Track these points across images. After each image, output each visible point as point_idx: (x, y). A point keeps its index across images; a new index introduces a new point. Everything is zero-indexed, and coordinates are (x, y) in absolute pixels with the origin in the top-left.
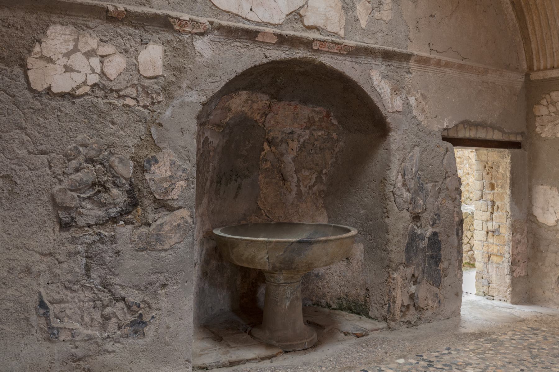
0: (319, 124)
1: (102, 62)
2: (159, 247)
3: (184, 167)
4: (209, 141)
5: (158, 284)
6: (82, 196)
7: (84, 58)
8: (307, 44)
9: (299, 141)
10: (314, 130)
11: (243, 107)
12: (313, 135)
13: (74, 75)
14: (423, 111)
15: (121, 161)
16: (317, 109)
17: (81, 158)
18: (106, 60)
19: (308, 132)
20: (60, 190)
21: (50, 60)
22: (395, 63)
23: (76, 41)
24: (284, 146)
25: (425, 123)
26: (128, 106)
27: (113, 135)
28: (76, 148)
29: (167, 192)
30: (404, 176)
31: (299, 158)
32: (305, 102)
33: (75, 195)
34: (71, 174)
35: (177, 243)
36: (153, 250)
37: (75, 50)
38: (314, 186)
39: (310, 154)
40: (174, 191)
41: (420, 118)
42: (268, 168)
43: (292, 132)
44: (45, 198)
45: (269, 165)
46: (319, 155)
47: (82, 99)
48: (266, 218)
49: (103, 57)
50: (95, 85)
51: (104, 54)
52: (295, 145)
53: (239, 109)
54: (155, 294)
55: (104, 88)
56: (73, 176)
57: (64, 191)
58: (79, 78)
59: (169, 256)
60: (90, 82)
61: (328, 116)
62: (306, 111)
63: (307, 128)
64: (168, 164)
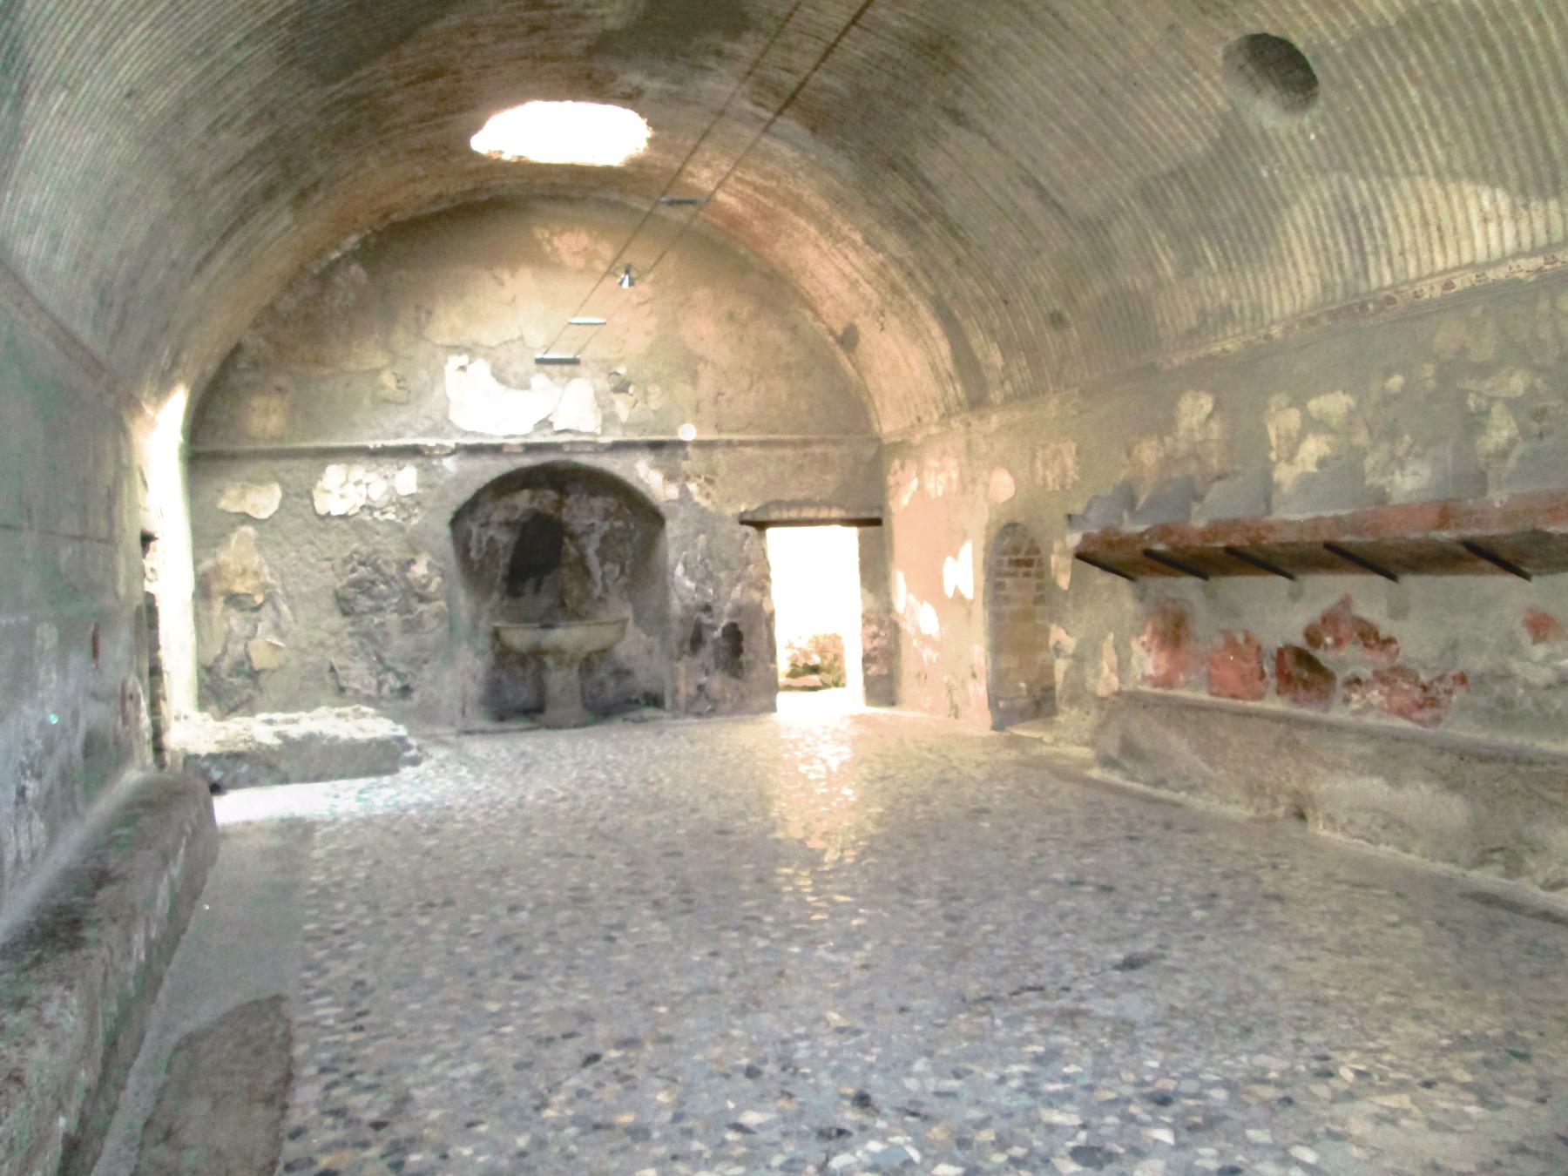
14: (708, 496)
21: (328, 492)
22: (666, 452)
25: (712, 509)
29: (425, 586)
41: (704, 503)
44: (331, 592)
52: (596, 537)
53: (528, 506)
54: (419, 669)
57: (344, 587)
61: (620, 506)
62: (598, 503)
63: (605, 519)
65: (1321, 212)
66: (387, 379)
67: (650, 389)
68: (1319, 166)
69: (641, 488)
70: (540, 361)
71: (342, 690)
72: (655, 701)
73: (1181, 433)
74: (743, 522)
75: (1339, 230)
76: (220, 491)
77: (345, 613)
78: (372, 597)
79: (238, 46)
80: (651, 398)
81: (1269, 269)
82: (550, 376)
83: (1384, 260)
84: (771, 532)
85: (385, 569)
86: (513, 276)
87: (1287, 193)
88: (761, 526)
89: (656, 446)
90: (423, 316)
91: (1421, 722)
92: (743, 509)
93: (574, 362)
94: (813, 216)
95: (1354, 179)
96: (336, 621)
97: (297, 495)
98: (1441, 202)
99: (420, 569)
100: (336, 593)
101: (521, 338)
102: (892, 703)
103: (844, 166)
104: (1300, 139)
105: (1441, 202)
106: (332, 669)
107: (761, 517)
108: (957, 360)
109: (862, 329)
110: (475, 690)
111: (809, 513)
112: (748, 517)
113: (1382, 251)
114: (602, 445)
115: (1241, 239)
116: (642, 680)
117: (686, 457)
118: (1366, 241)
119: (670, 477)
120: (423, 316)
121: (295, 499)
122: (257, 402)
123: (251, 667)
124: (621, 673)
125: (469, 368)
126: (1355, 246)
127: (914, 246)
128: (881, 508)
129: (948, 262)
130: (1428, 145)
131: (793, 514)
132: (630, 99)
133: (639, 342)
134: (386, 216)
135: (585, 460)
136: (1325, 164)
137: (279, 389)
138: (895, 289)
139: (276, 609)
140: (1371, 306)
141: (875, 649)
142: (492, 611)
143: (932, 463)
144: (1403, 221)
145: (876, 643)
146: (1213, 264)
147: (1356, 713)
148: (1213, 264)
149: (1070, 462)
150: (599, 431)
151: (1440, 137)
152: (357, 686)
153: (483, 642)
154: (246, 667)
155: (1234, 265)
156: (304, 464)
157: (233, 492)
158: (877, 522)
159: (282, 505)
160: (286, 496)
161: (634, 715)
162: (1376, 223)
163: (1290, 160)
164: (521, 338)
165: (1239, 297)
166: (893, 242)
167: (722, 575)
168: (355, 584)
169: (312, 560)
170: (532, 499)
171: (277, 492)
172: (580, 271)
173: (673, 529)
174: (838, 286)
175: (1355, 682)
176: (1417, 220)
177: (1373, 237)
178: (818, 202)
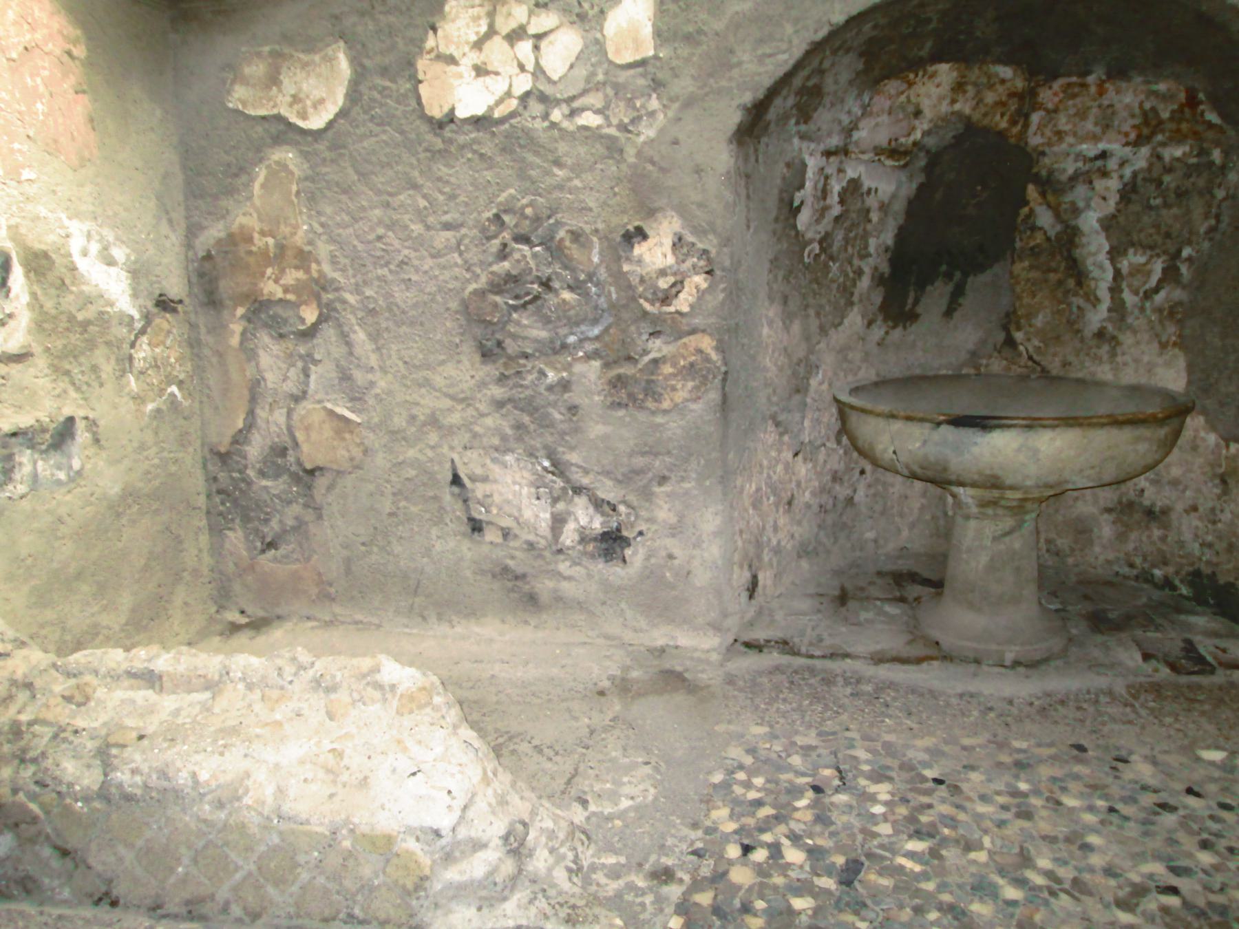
0: (1171, 126)
1: (536, 48)
2: (650, 404)
3: (700, 246)
4: (865, 188)
5: (650, 475)
6: (511, 302)
7: (505, 45)
9: (1121, 177)
10: (1163, 144)
11: (953, 101)
12: (1159, 157)
13: (488, 80)
16: (1162, 87)
17: (506, 235)
18: (544, 44)
19: (1145, 151)
20: (475, 292)
21: (451, 60)
26: (586, 128)
27: (560, 187)
28: (497, 217)
31: (1121, 219)
33: (498, 299)
34: (490, 264)
35: (687, 400)
36: (642, 408)
37: (491, 32)
38: (1156, 290)
39: (1150, 208)
40: (681, 296)
42: (1038, 246)
46: (1175, 211)
47: (507, 126)
48: (1030, 363)
49: (539, 37)
50: (527, 94)
51: (541, 31)
54: (647, 494)
55: (543, 98)
56: (495, 268)
58: (498, 86)
60: (518, 91)
64: (668, 242)
106: (456, 480)
139: (345, 339)
142: (843, 351)
159: (354, 95)
169: (417, 228)
171: (344, 65)
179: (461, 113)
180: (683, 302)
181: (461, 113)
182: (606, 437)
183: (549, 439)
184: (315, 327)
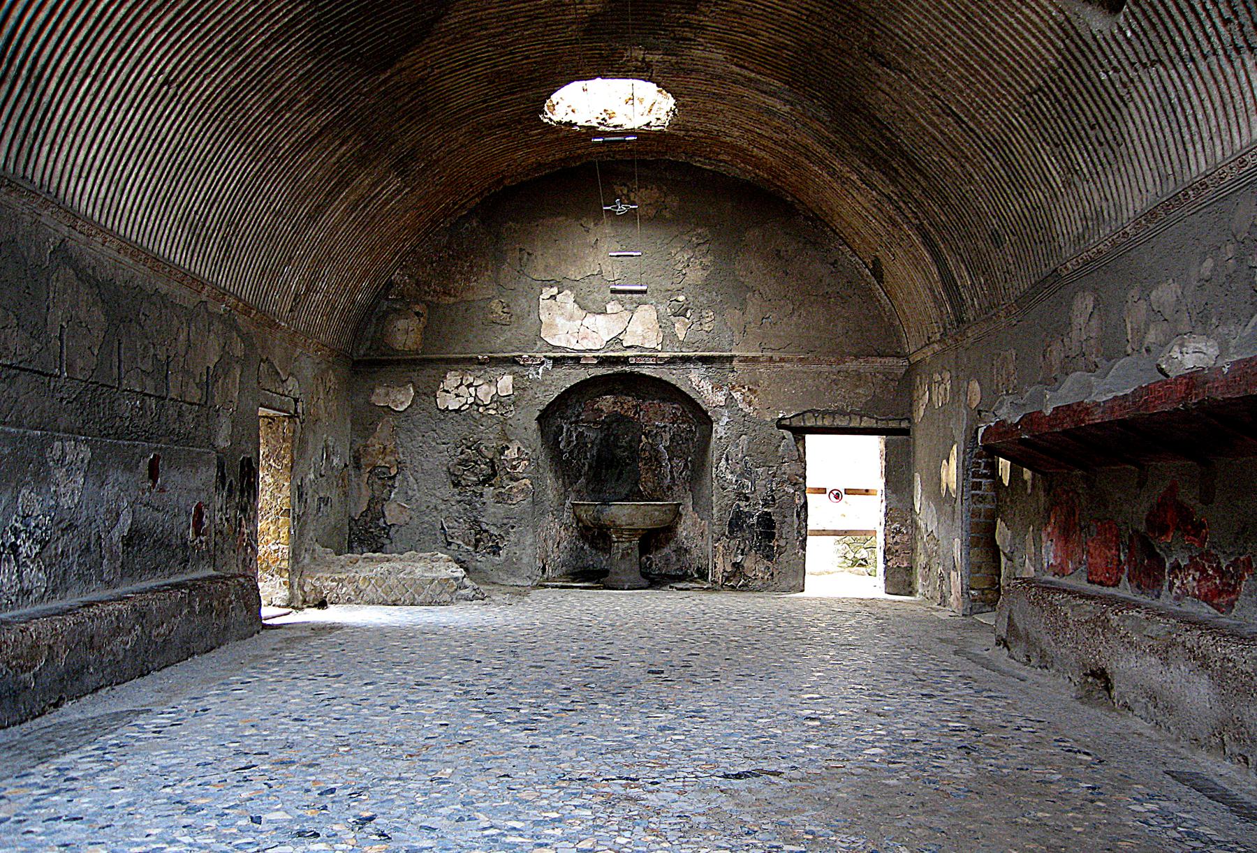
2: (510, 502)
8: (624, 361)
14: (750, 404)
15: (486, 448)
23: (462, 379)
24: (659, 438)
29: (515, 467)
30: (727, 460)
32: (664, 400)
37: (461, 384)
43: (665, 426)
44: (445, 469)
45: (647, 453)
54: (508, 533)
59: (516, 509)
61: (684, 411)
62: (668, 408)
65: (1150, 106)
66: (495, 305)
67: (704, 313)
68: (1140, 61)
69: (693, 395)
70: (613, 292)
71: (449, 544)
72: (703, 575)
73: (1074, 334)
74: (780, 426)
75: (1164, 123)
76: (373, 390)
77: (456, 485)
78: (476, 475)
79: (265, 45)
80: (703, 321)
81: (1122, 169)
82: (620, 302)
83: (1199, 146)
84: (808, 437)
85: (486, 453)
86: (596, 225)
87: (1123, 92)
88: (800, 433)
89: (704, 360)
90: (526, 256)
91: (1218, 607)
92: (780, 416)
93: (645, 292)
94: (821, 162)
95: (1165, 68)
96: (448, 491)
97: (425, 394)
98: (1232, 80)
99: (512, 453)
100: (449, 469)
101: (601, 272)
102: (911, 594)
103: (822, 114)
104: (1120, 37)
105: (1232, 80)
106: (443, 528)
107: (795, 423)
108: (944, 284)
109: (882, 260)
110: (557, 555)
111: (841, 422)
112: (787, 422)
113: (1196, 138)
114: (661, 359)
115: (1101, 144)
116: (695, 559)
117: (733, 371)
118: (1184, 130)
119: (717, 387)
120: (526, 256)
121: (423, 397)
122: (401, 324)
123: (385, 523)
124: (682, 551)
125: (558, 297)
126: (1177, 136)
127: (893, 181)
128: (909, 420)
129: (917, 193)
130: (1214, 25)
131: (827, 422)
132: (642, 72)
133: (695, 275)
134: (500, 182)
135: (646, 371)
136: (1145, 60)
137: (417, 314)
138: (894, 224)
140: (1191, 193)
141: (896, 543)
143: (937, 377)
144: (1208, 104)
145: (897, 538)
146: (1085, 170)
147: (1177, 598)
148: (1085, 170)
149: (1011, 367)
150: (659, 348)
151: (1221, 15)
152: (460, 542)
153: (567, 517)
154: (381, 522)
155: (1099, 168)
156: (429, 371)
157: (380, 391)
158: (906, 432)
160: (416, 392)
161: (680, 585)
162: (1189, 111)
163: (1120, 62)
164: (601, 272)
165: (1107, 200)
166: (876, 177)
167: (760, 470)
168: (464, 463)
169: (434, 444)
170: (615, 403)
172: (650, 220)
173: (719, 430)
174: (857, 223)
175: (1176, 567)
176: (1218, 104)
177: (1188, 126)
178: (821, 150)
179: (450, 408)
180: (519, 469)
181: (450, 408)
182: (494, 513)
183: (475, 513)
184: (395, 476)
